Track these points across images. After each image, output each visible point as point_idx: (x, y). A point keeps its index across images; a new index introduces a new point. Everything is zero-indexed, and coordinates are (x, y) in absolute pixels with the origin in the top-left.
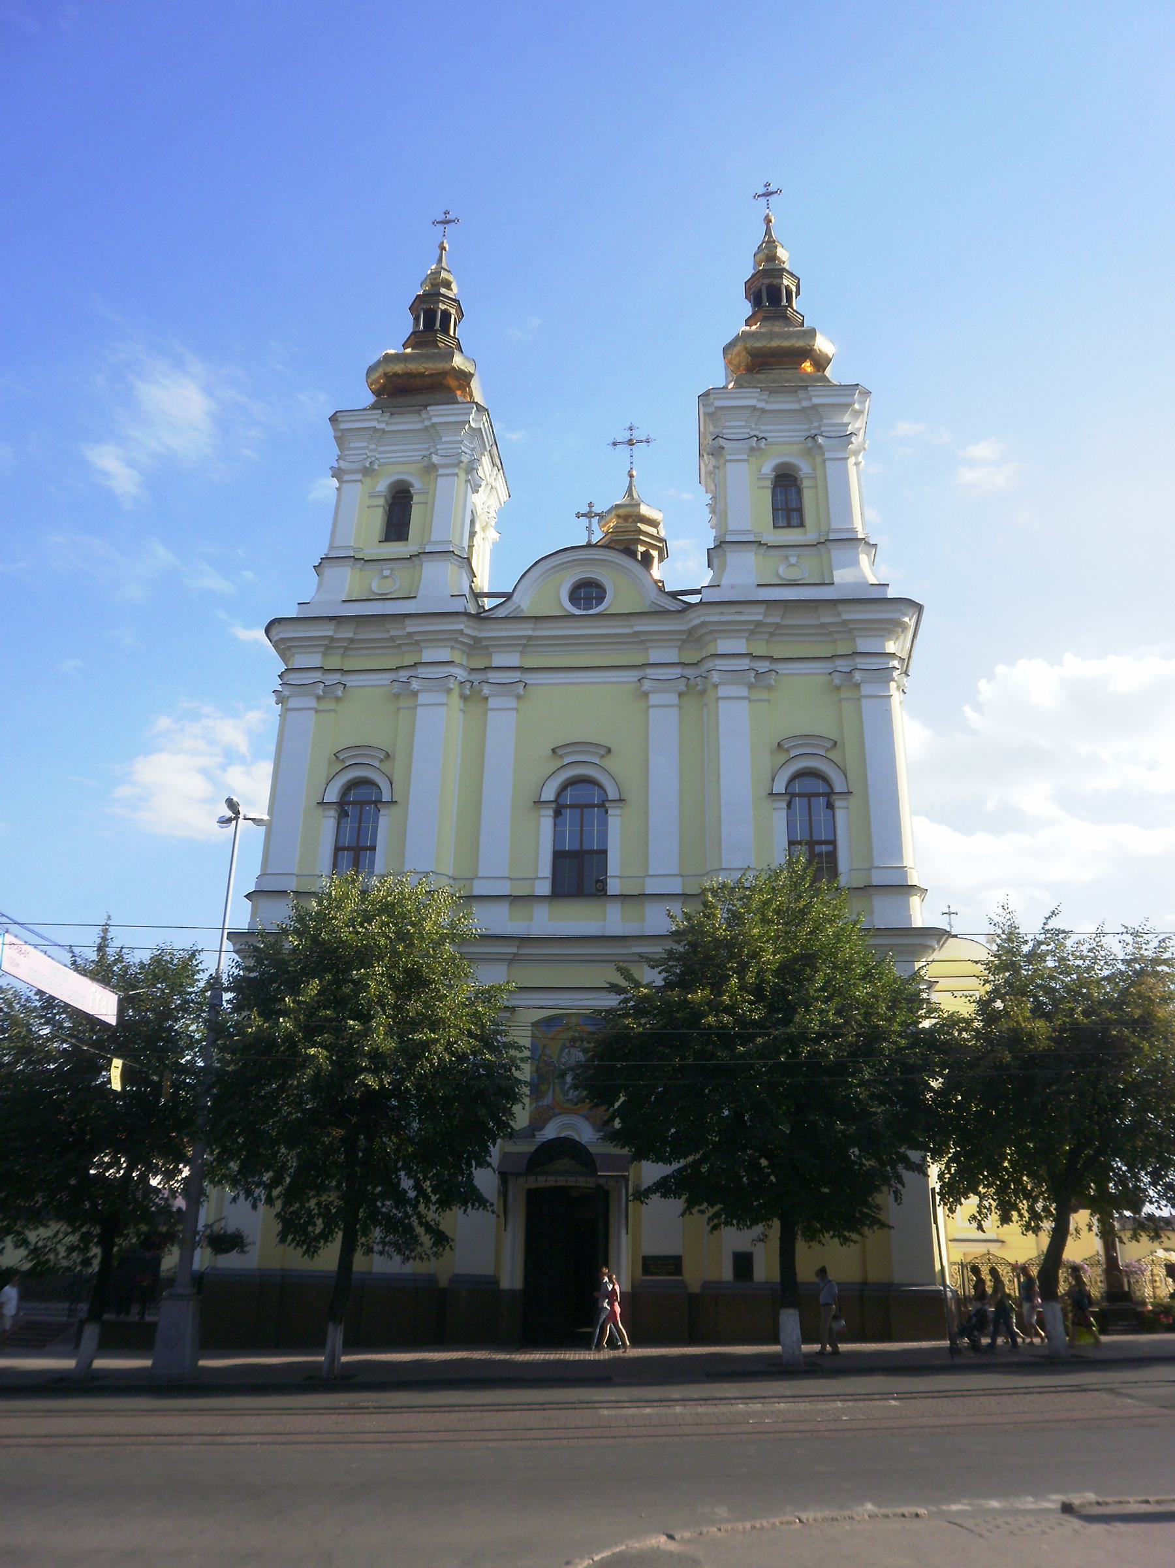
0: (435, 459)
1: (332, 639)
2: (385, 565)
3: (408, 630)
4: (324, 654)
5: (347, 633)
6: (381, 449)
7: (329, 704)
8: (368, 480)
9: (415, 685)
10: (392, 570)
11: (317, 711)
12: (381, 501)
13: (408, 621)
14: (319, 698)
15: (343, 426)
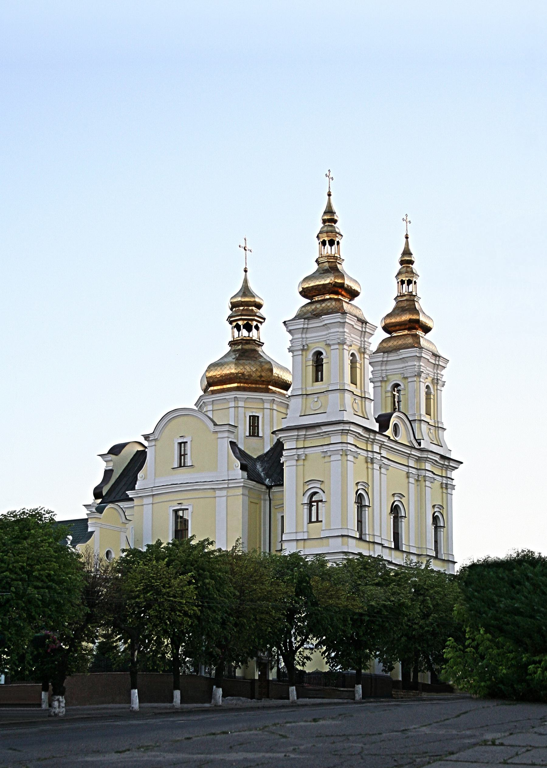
0: (328, 342)
1: (298, 435)
2: (316, 396)
3: (324, 430)
4: (297, 441)
5: (303, 433)
6: (308, 336)
7: (301, 462)
8: (304, 353)
9: (329, 454)
10: (318, 398)
11: (297, 466)
12: (311, 363)
13: (323, 428)
14: (297, 460)
15: (290, 328)
